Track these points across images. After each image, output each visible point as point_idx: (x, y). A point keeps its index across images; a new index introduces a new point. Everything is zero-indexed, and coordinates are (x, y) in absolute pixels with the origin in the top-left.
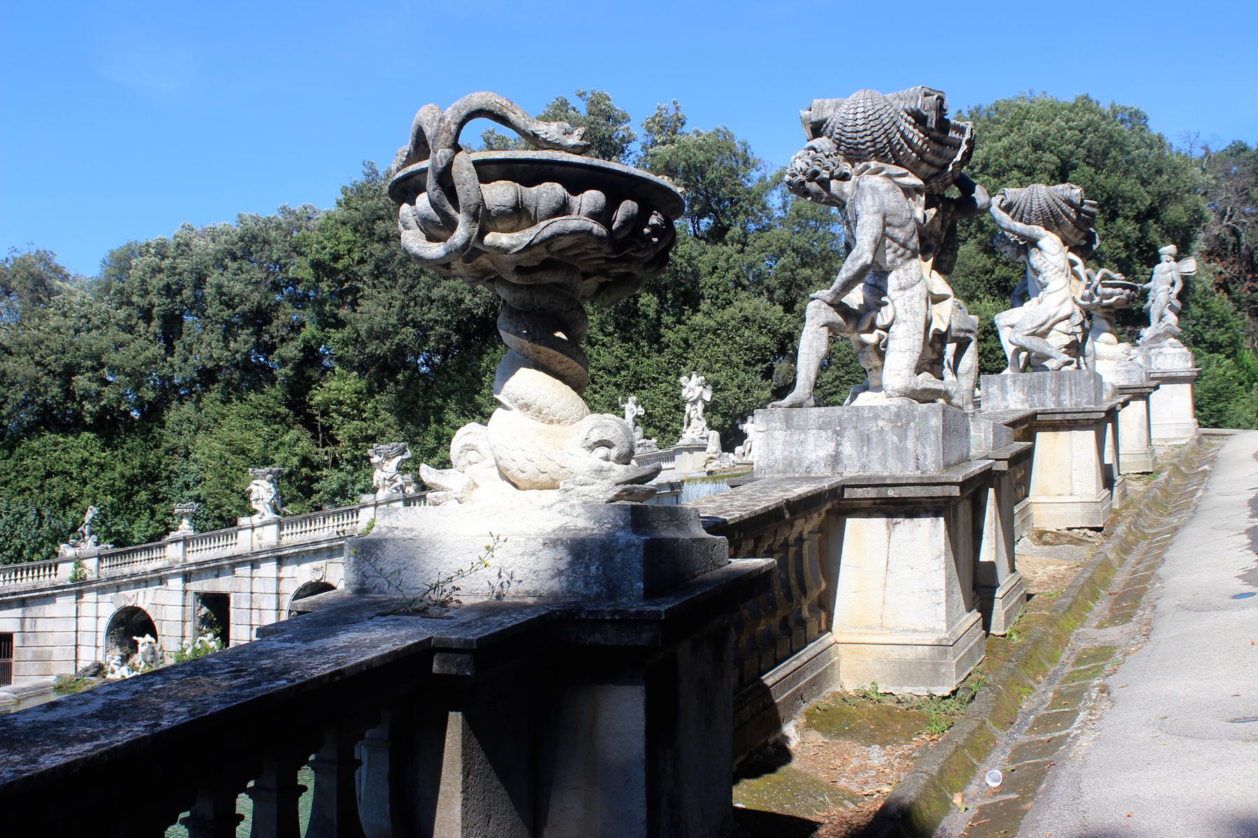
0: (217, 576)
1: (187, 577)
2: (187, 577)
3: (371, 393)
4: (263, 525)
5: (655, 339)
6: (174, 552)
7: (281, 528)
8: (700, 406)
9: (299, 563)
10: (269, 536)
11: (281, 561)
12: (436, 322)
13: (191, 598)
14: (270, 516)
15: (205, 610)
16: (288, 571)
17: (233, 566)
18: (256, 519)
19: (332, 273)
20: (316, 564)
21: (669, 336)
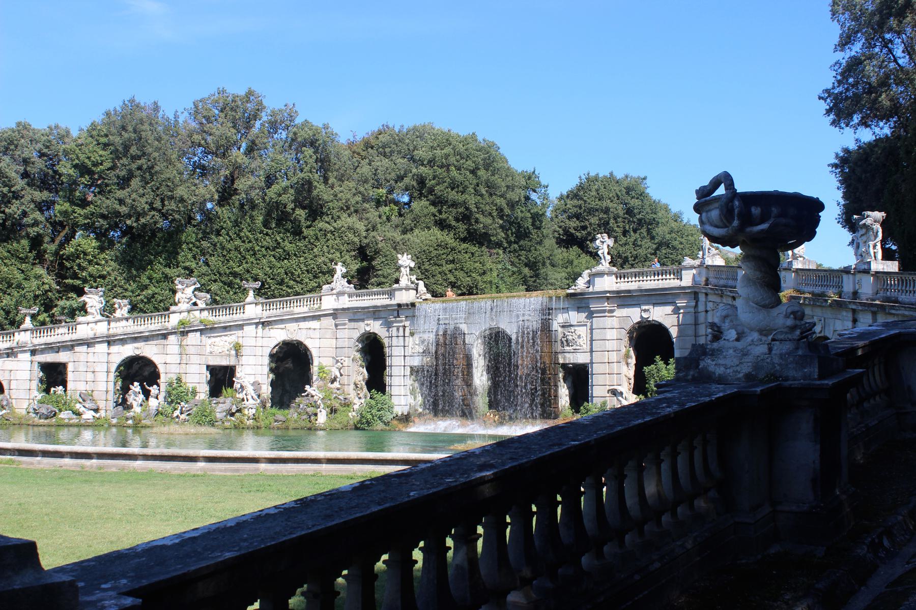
0: (58, 352)
1: (33, 352)
2: (33, 352)
3: (102, 249)
4: (96, 322)
5: (297, 232)
6: (22, 337)
7: (109, 324)
8: (408, 269)
9: (123, 344)
10: (102, 328)
11: (109, 343)
12: (173, 210)
13: (36, 366)
14: (99, 317)
15: (41, 374)
16: (115, 349)
17: (72, 347)
18: (89, 318)
19: (90, 173)
20: (136, 345)
21: (306, 232)
